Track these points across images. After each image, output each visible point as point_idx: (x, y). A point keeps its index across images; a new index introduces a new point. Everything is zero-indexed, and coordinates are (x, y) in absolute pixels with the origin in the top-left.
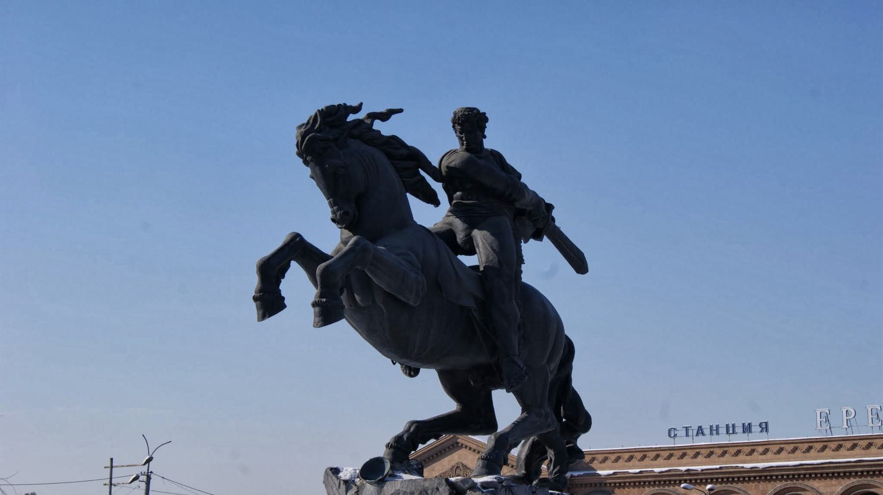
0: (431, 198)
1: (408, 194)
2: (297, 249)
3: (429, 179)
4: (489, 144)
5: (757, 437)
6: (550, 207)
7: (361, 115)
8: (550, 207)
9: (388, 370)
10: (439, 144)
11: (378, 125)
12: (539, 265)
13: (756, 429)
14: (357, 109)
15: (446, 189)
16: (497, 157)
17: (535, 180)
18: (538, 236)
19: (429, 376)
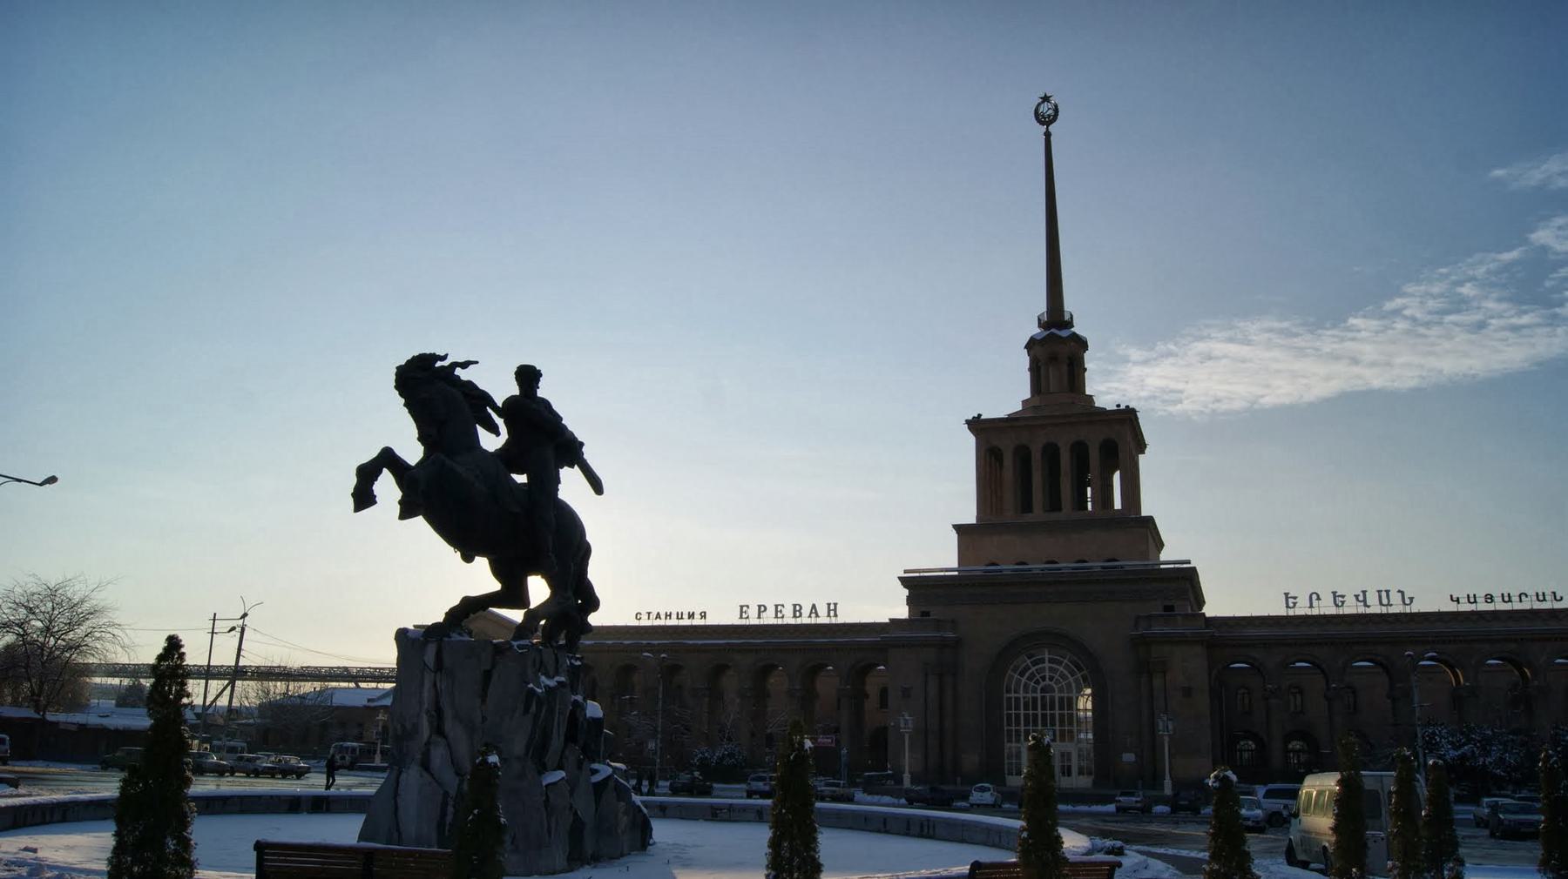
0: (494, 430)
1: (479, 428)
2: (388, 459)
4: (540, 393)
5: (697, 621)
6: (582, 444)
7: (446, 363)
8: (582, 444)
9: (452, 555)
10: (502, 388)
11: (458, 371)
12: (571, 486)
13: (697, 616)
14: (444, 358)
16: (546, 404)
17: (573, 421)
18: (572, 466)
19: (482, 563)
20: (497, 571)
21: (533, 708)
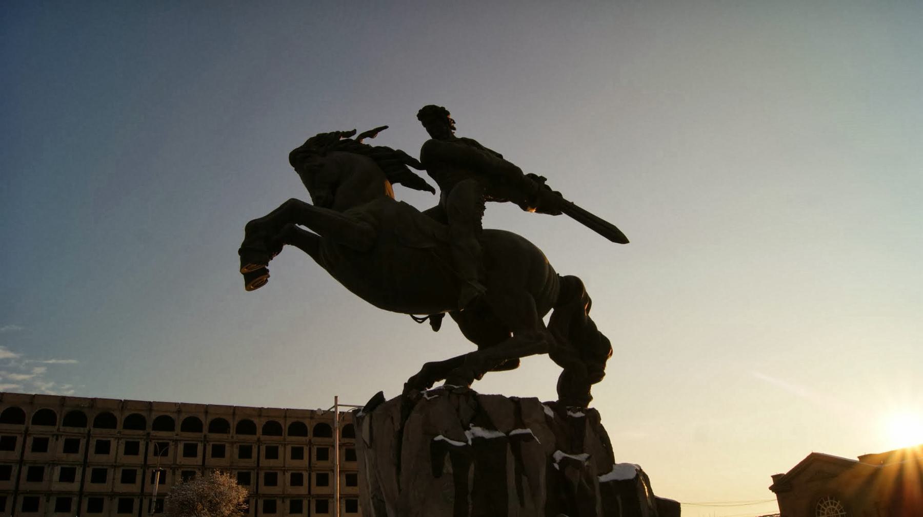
0: (420, 185)
3: (413, 170)
4: (458, 134)
7: (354, 138)
11: (366, 141)
15: (430, 174)
20: (469, 333)
21: (448, 468)
